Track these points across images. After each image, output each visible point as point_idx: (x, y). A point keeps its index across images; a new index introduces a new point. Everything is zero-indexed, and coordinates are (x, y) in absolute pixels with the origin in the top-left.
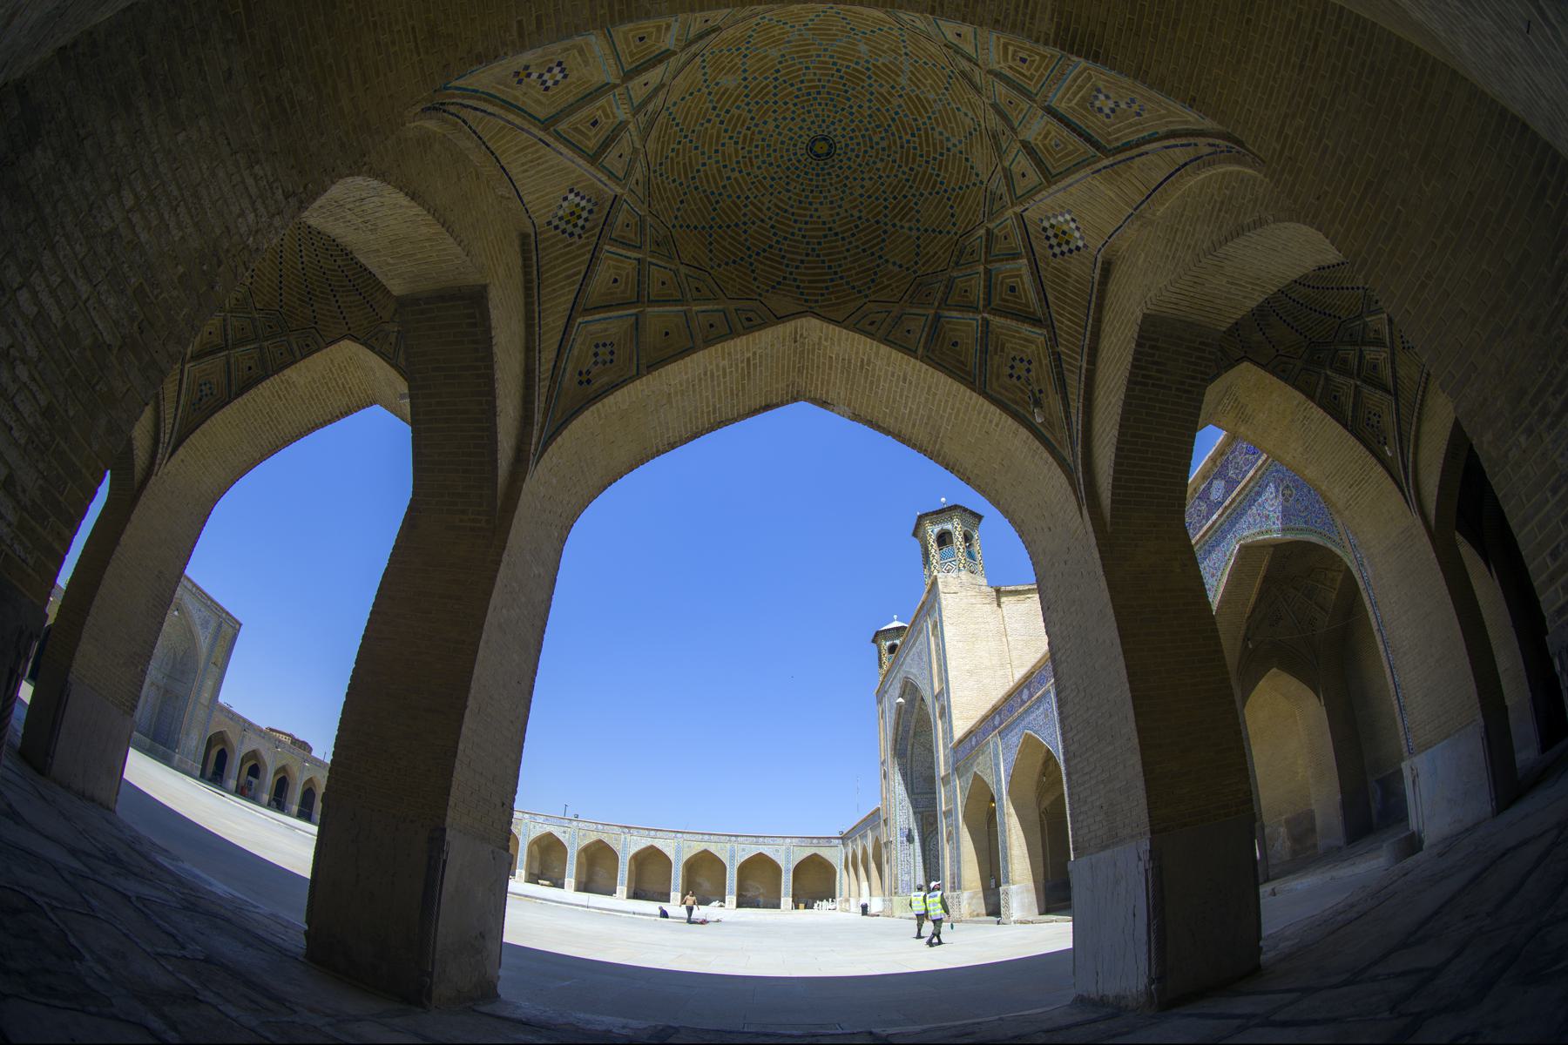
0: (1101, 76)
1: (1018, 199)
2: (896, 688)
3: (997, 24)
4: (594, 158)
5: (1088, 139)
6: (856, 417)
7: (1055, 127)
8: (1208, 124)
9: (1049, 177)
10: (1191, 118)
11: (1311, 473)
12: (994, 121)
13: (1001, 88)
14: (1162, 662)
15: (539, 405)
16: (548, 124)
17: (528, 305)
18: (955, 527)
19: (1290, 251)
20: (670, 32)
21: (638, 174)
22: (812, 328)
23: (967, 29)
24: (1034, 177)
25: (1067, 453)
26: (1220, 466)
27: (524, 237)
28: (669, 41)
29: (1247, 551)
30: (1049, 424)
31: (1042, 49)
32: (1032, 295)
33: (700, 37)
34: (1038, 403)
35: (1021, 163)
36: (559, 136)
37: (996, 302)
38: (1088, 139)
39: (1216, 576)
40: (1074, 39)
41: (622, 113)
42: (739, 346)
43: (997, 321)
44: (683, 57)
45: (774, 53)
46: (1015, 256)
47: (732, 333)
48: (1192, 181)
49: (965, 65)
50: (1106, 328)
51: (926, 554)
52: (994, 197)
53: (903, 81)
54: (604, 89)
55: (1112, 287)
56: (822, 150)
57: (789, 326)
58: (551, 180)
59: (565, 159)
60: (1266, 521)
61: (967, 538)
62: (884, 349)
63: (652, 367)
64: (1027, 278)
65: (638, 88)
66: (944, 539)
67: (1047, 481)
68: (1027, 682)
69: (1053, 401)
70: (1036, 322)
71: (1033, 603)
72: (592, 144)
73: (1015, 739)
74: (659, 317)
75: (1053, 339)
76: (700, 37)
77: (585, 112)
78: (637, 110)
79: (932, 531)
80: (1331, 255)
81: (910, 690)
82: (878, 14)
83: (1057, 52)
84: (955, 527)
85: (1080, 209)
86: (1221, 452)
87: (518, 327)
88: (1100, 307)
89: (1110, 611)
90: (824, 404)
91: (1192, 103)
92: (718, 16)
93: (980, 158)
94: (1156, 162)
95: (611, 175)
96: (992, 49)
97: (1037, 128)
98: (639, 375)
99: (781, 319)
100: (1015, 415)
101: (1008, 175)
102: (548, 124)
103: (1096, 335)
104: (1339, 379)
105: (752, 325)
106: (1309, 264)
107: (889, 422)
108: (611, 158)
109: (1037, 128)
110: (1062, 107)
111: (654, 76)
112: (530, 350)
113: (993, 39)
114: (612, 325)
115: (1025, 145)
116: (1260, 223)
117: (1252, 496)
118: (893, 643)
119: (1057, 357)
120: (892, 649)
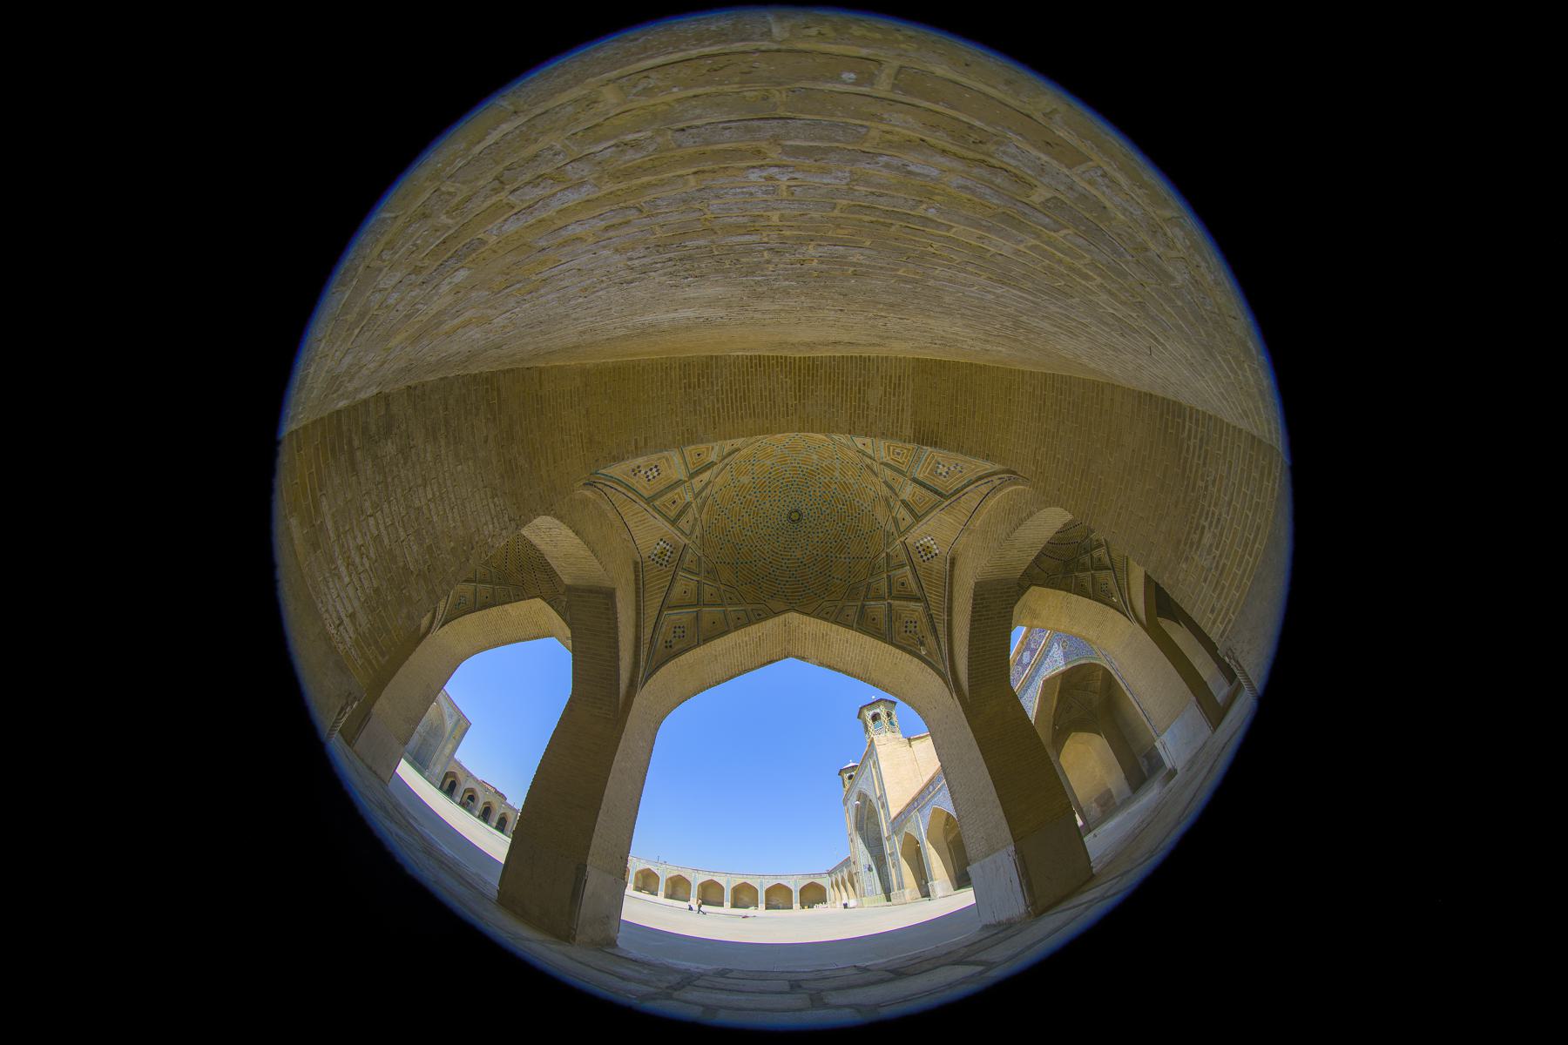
0: (939, 454)
1: (901, 534)
2: (855, 796)
3: (883, 435)
4: (673, 522)
5: (936, 492)
6: (821, 664)
7: (918, 489)
8: (997, 467)
9: (918, 518)
10: (988, 467)
11: (1075, 630)
12: (885, 491)
13: (888, 472)
14: (1007, 756)
15: (643, 656)
16: (649, 501)
17: (638, 602)
18: (881, 710)
19: (1050, 521)
20: (713, 450)
21: (698, 531)
22: (794, 618)
23: (868, 441)
24: (909, 519)
25: (941, 667)
26: (1026, 645)
27: (636, 563)
28: (713, 457)
29: (1048, 683)
30: (929, 653)
31: (910, 446)
32: (914, 586)
33: (729, 454)
34: (922, 644)
35: (903, 513)
36: (655, 508)
37: (894, 593)
38: (936, 492)
39: (1031, 703)
40: (925, 437)
41: (689, 497)
42: (754, 629)
43: (896, 603)
44: (721, 466)
45: (768, 463)
46: (903, 565)
47: (750, 623)
48: (992, 502)
49: (869, 461)
50: (956, 595)
51: (866, 726)
52: (889, 534)
53: (837, 474)
54: (679, 483)
55: (956, 572)
56: (796, 517)
57: (781, 618)
58: (651, 533)
59: (660, 522)
60: (1056, 663)
61: (889, 715)
62: (835, 627)
63: (706, 641)
64: (910, 576)
65: (697, 483)
66: (875, 717)
67: (932, 684)
68: (931, 782)
69: (930, 640)
70: (917, 600)
71: (929, 741)
72: (672, 514)
73: (928, 811)
74: (710, 613)
75: (928, 607)
76: (729, 454)
77: (669, 495)
78: (696, 496)
79: (868, 714)
80: (1070, 517)
81: (863, 797)
82: (820, 436)
83: (915, 445)
84: (881, 710)
85: (935, 533)
86: (1025, 637)
87: (631, 613)
88: (951, 584)
89: (974, 743)
90: (803, 658)
91: (987, 458)
92: (738, 442)
93: (880, 513)
94: (971, 499)
95: (683, 533)
96: (881, 449)
97: (908, 491)
98: (698, 645)
99: (776, 614)
100: (910, 652)
101: (895, 521)
102: (649, 501)
103: (951, 599)
104: (1081, 575)
105: (760, 618)
106: (1059, 525)
107: (840, 665)
108: (682, 523)
109: (908, 491)
110: (920, 477)
111: (706, 476)
112: (638, 626)
113: (882, 444)
114: (683, 617)
115: (903, 502)
116: (1031, 514)
117: (1046, 653)
118: (851, 774)
119: (931, 616)
120: (850, 777)
